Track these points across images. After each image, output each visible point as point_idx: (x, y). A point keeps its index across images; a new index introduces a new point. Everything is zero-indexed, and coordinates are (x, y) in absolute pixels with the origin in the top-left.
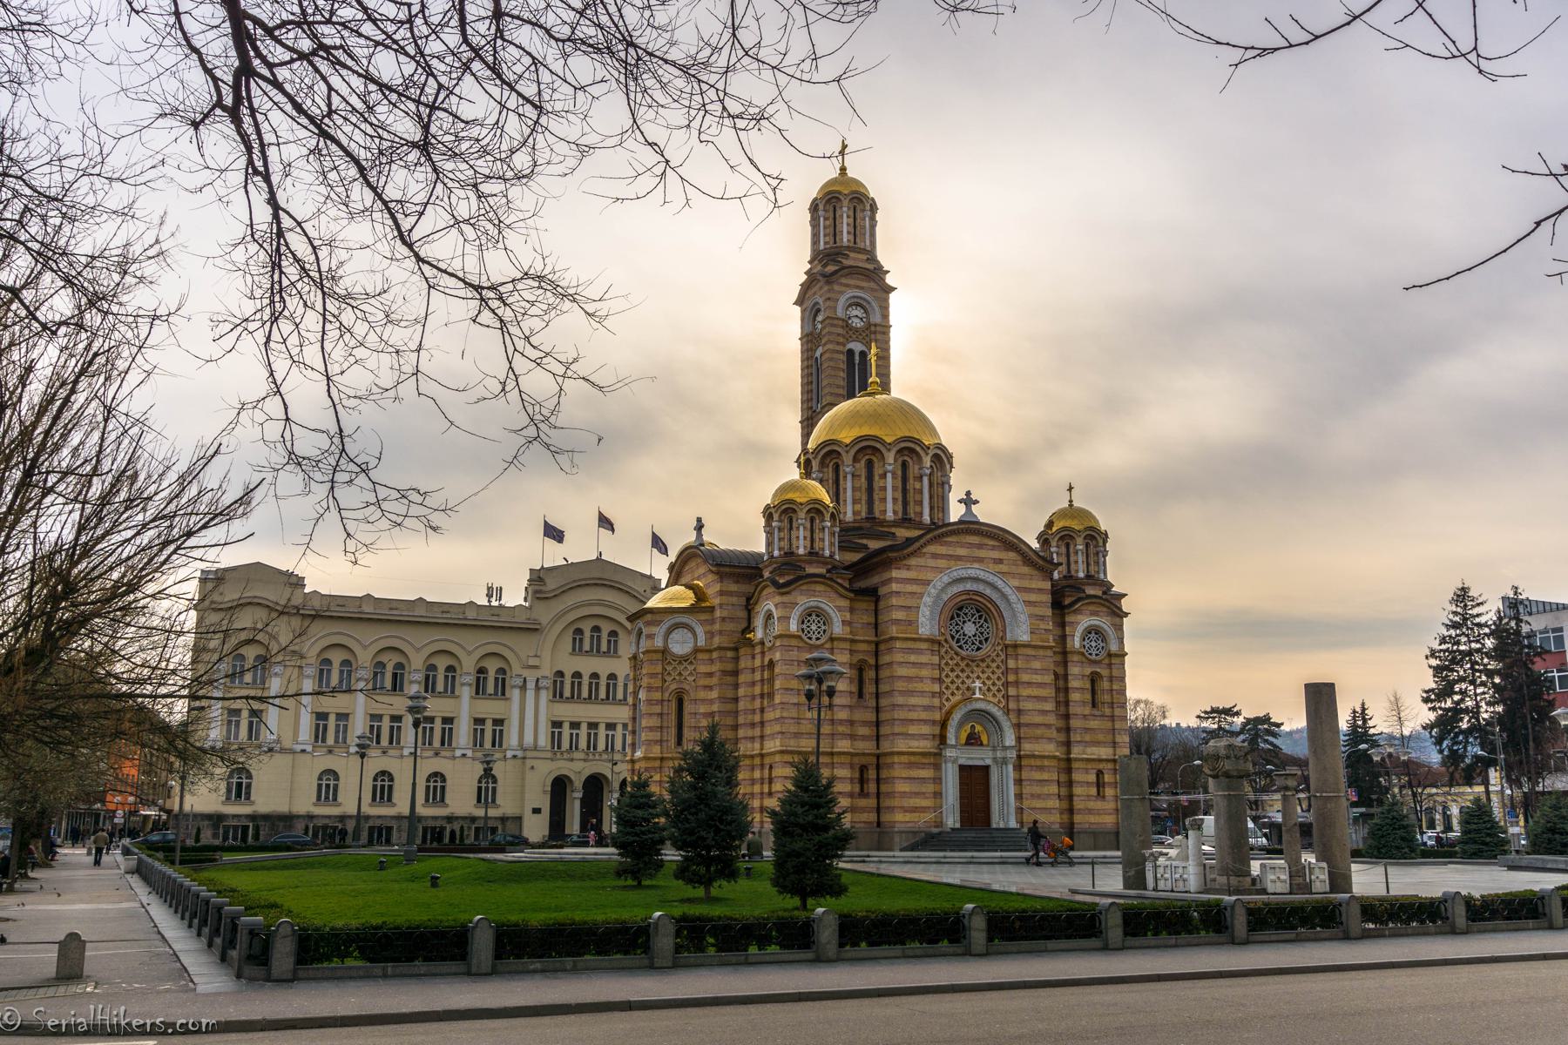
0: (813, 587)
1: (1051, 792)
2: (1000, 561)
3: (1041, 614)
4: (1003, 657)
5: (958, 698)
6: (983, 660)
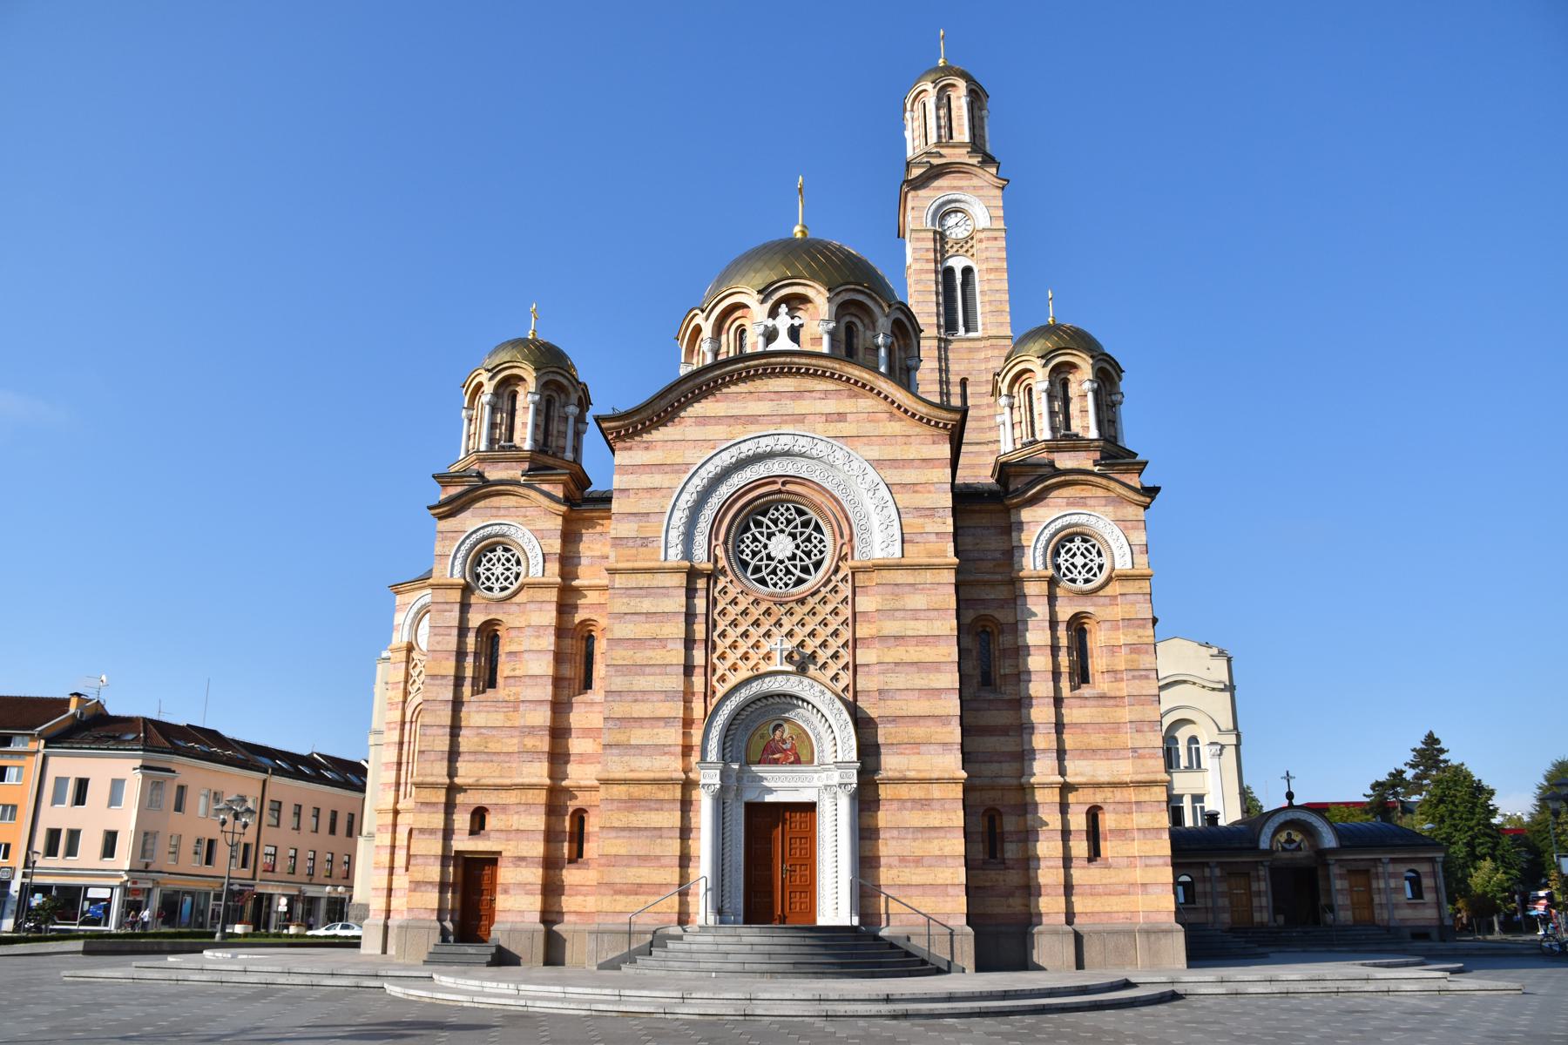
0: (495, 501)
1: (947, 851)
2: (841, 417)
3: (928, 504)
4: (846, 590)
5: (744, 673)
6: (802, 601)
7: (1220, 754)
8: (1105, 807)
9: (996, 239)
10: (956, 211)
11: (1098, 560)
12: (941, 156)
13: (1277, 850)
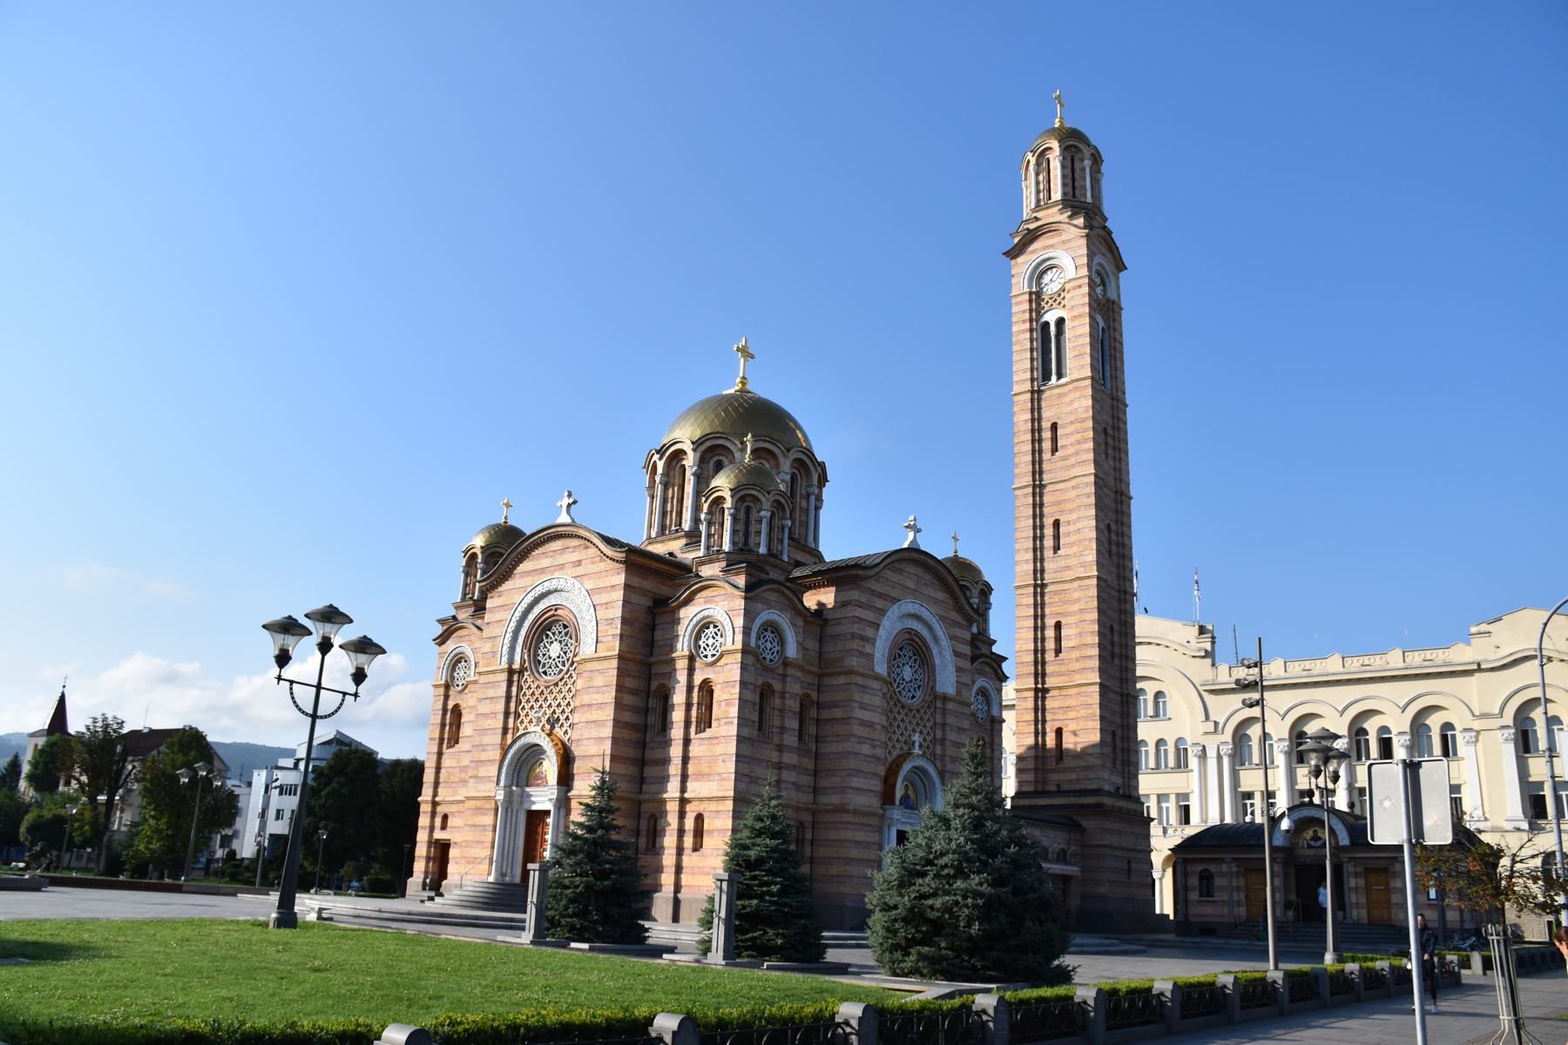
2: (579, 563)
6: (556, 684)
7: (1477, 741)
8: (705, 814)
9: (1080, 286)
10: (1051, 268)
11: (720, 640)
12: (1037, 219)
13: (1303, 847)
